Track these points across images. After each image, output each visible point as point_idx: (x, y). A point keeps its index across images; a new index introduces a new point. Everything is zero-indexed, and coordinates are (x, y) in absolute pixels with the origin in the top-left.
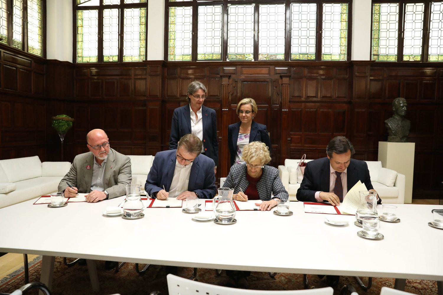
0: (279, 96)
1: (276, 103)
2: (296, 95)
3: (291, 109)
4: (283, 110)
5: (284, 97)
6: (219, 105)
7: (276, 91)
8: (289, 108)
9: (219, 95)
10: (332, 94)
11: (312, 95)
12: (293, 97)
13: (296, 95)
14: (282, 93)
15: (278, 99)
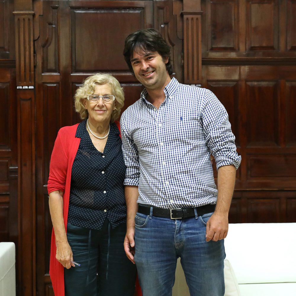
6: (9, 75)
14: (183, 40)
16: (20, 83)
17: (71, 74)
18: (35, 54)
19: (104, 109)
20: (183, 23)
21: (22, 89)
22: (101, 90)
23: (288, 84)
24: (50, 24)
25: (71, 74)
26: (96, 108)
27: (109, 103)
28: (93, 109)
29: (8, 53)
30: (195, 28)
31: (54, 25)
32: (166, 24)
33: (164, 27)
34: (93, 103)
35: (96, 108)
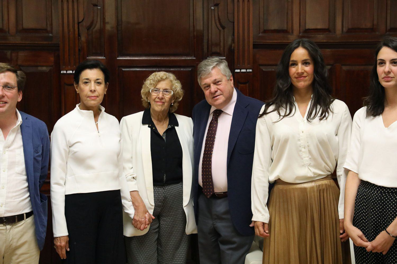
0: (226, 30)
1: (218, 51)
2: (274, 25)
3: (261, 67)
4: (239, 71)
5: (238, 33)
6: (52, 59)
7: (217, 18)
8: (255, 65)
9: (49, 29)
10: (375, 22)
11: (319, 27)
12: (265, 31)
13: (273, 28)
14: (234, 23)
15: (222, 38)
16: (64, 67)
17: (118, 58)
18: (80, 37)
19: (163, 101)
20: (234, 5)
21: (67, 74)
22: (162, 85)
23: (344, 68)
24: (95, 5)
25: (118, 58)
26: (157, 100)
27: (167, 97)
28: (154, 100)
29: (51, 36)
30: (246, 11)
31: (99, 7)
32: (216, 5)
33: (214, 9)
34: (154, 95)
35: (157, 100)
